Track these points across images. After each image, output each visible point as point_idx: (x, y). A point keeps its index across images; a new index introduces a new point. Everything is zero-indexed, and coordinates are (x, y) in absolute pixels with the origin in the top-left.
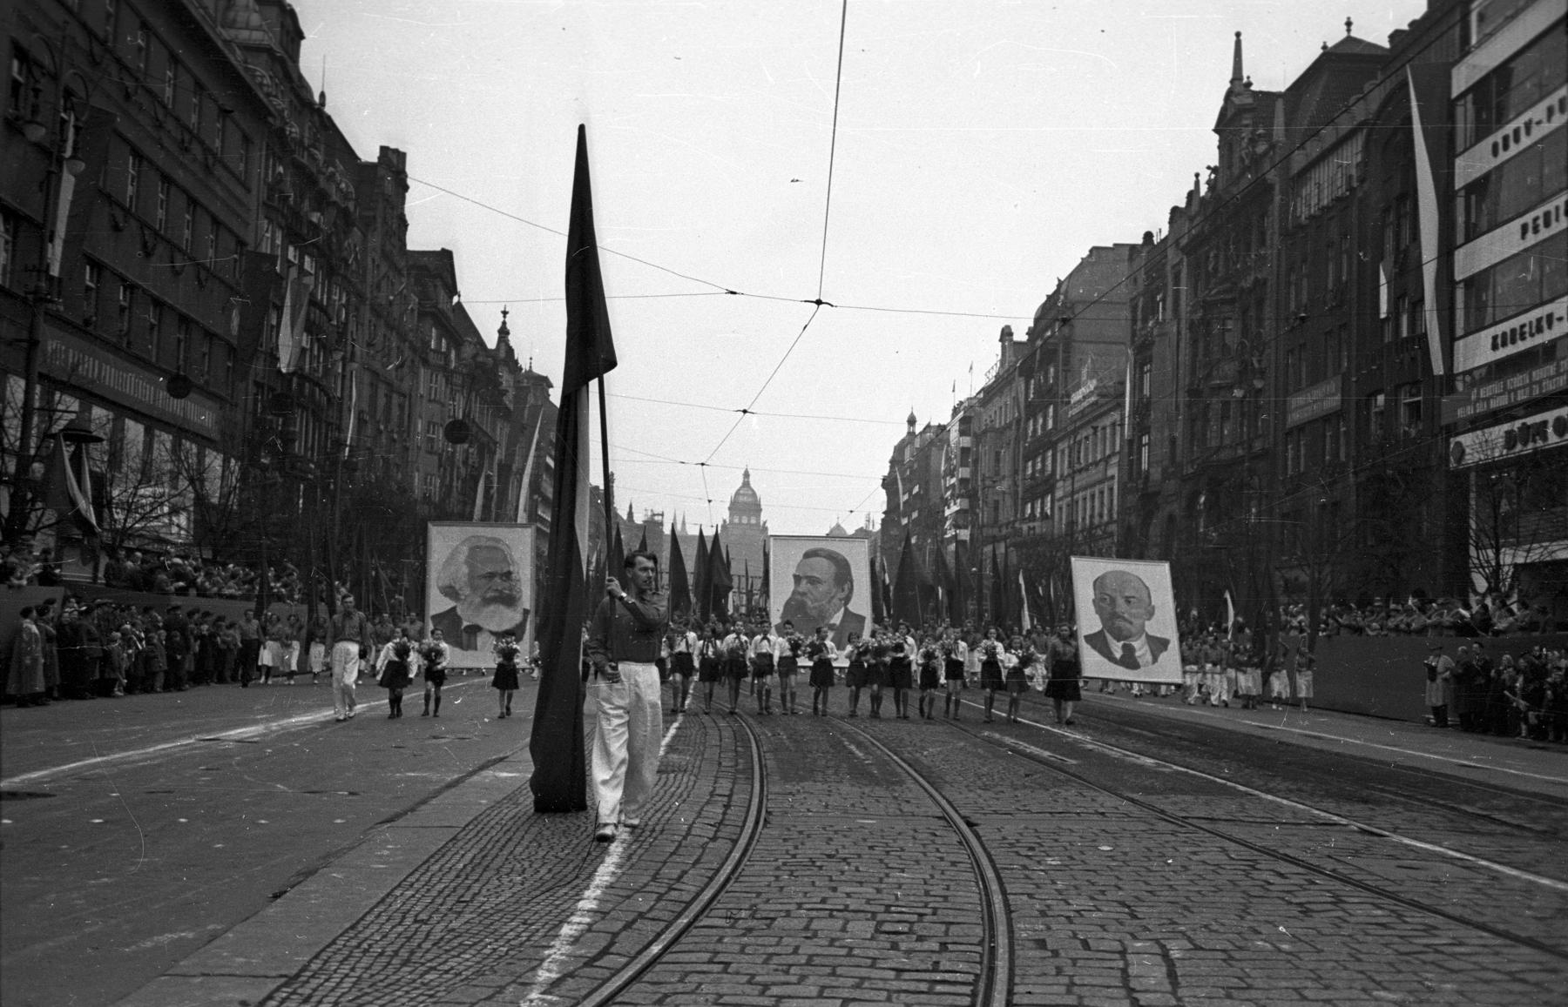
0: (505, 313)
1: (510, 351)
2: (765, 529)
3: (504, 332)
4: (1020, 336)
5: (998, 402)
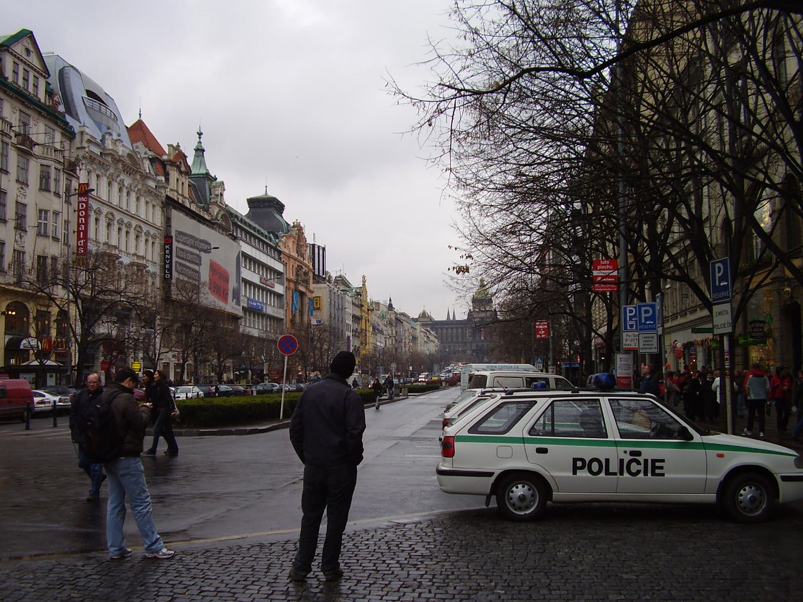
0: (200, 134)
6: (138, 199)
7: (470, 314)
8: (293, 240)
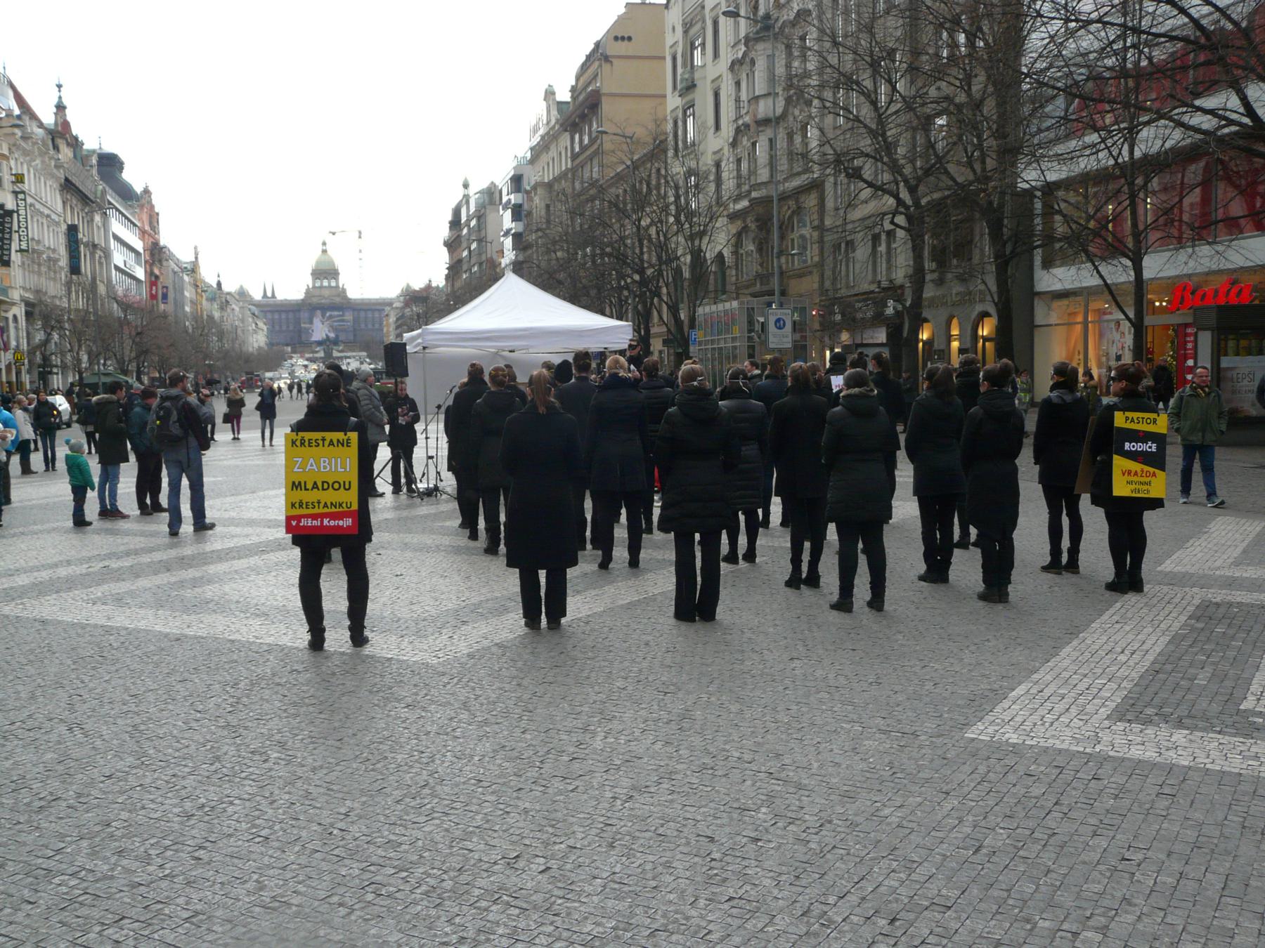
0: (59, 86)
1: (66, 125)
2: (344, 291)
3: (60, 108)
4: (564, 95)
5: (545, 158)
7: (308, 292)
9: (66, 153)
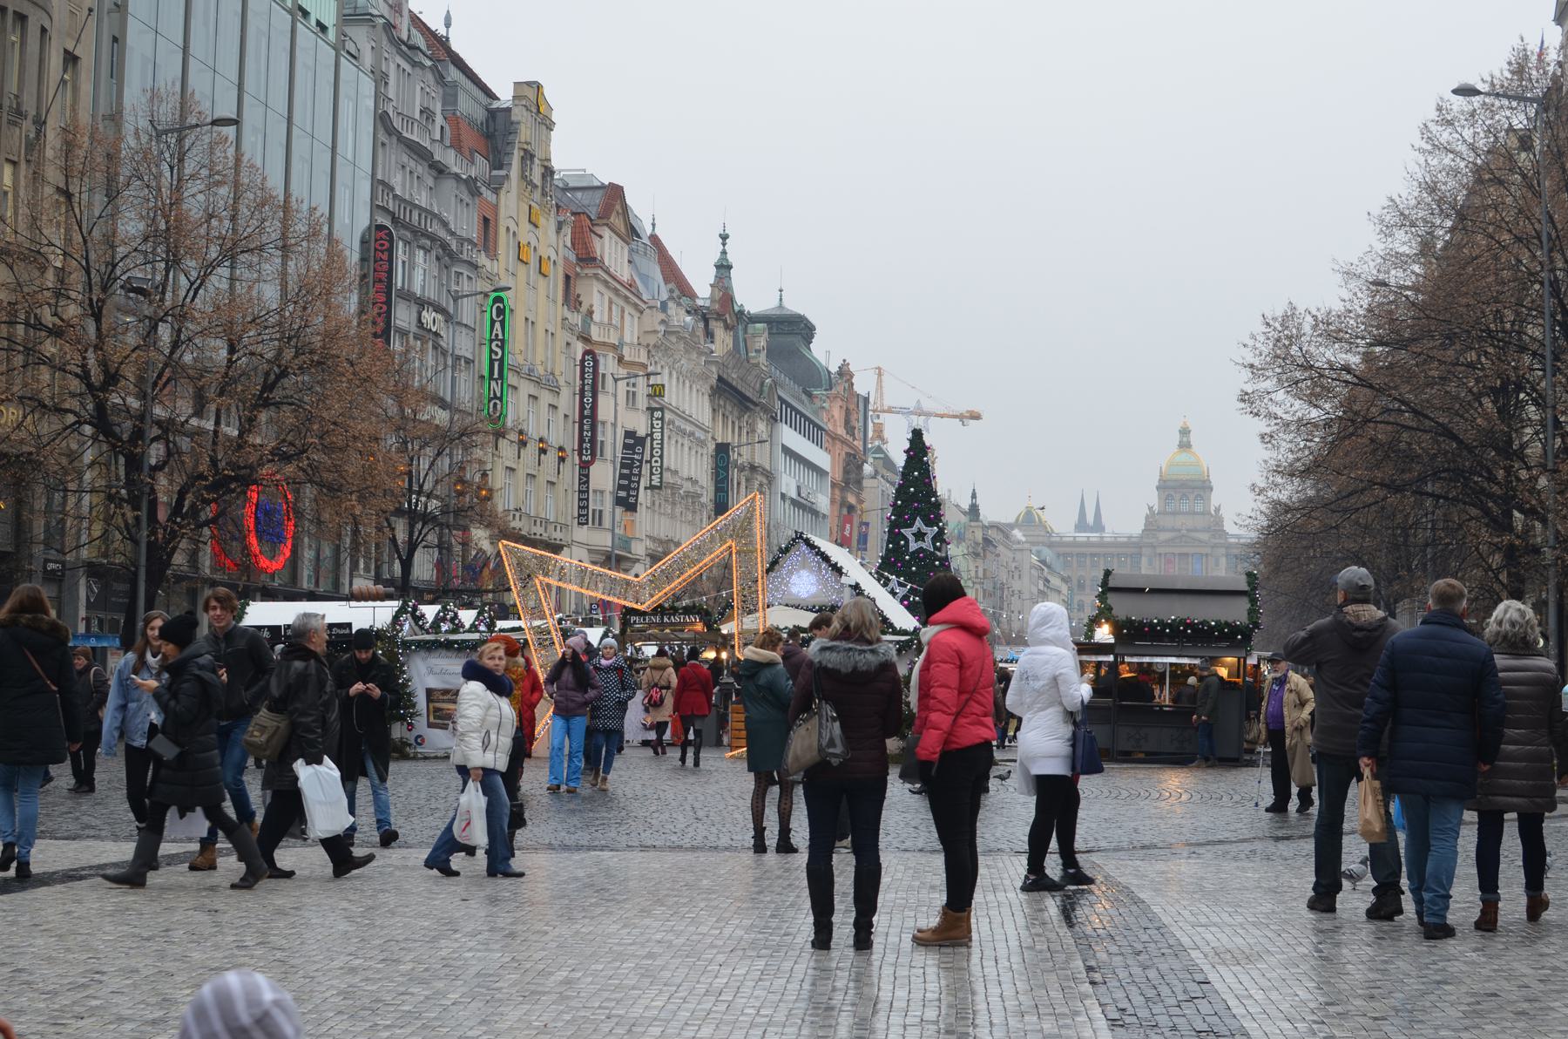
0: (724, 237)
2: (1219, 521)
3: (724, 267)
6: (691, 387)
8: (840, 403)
9: (722, 342)
